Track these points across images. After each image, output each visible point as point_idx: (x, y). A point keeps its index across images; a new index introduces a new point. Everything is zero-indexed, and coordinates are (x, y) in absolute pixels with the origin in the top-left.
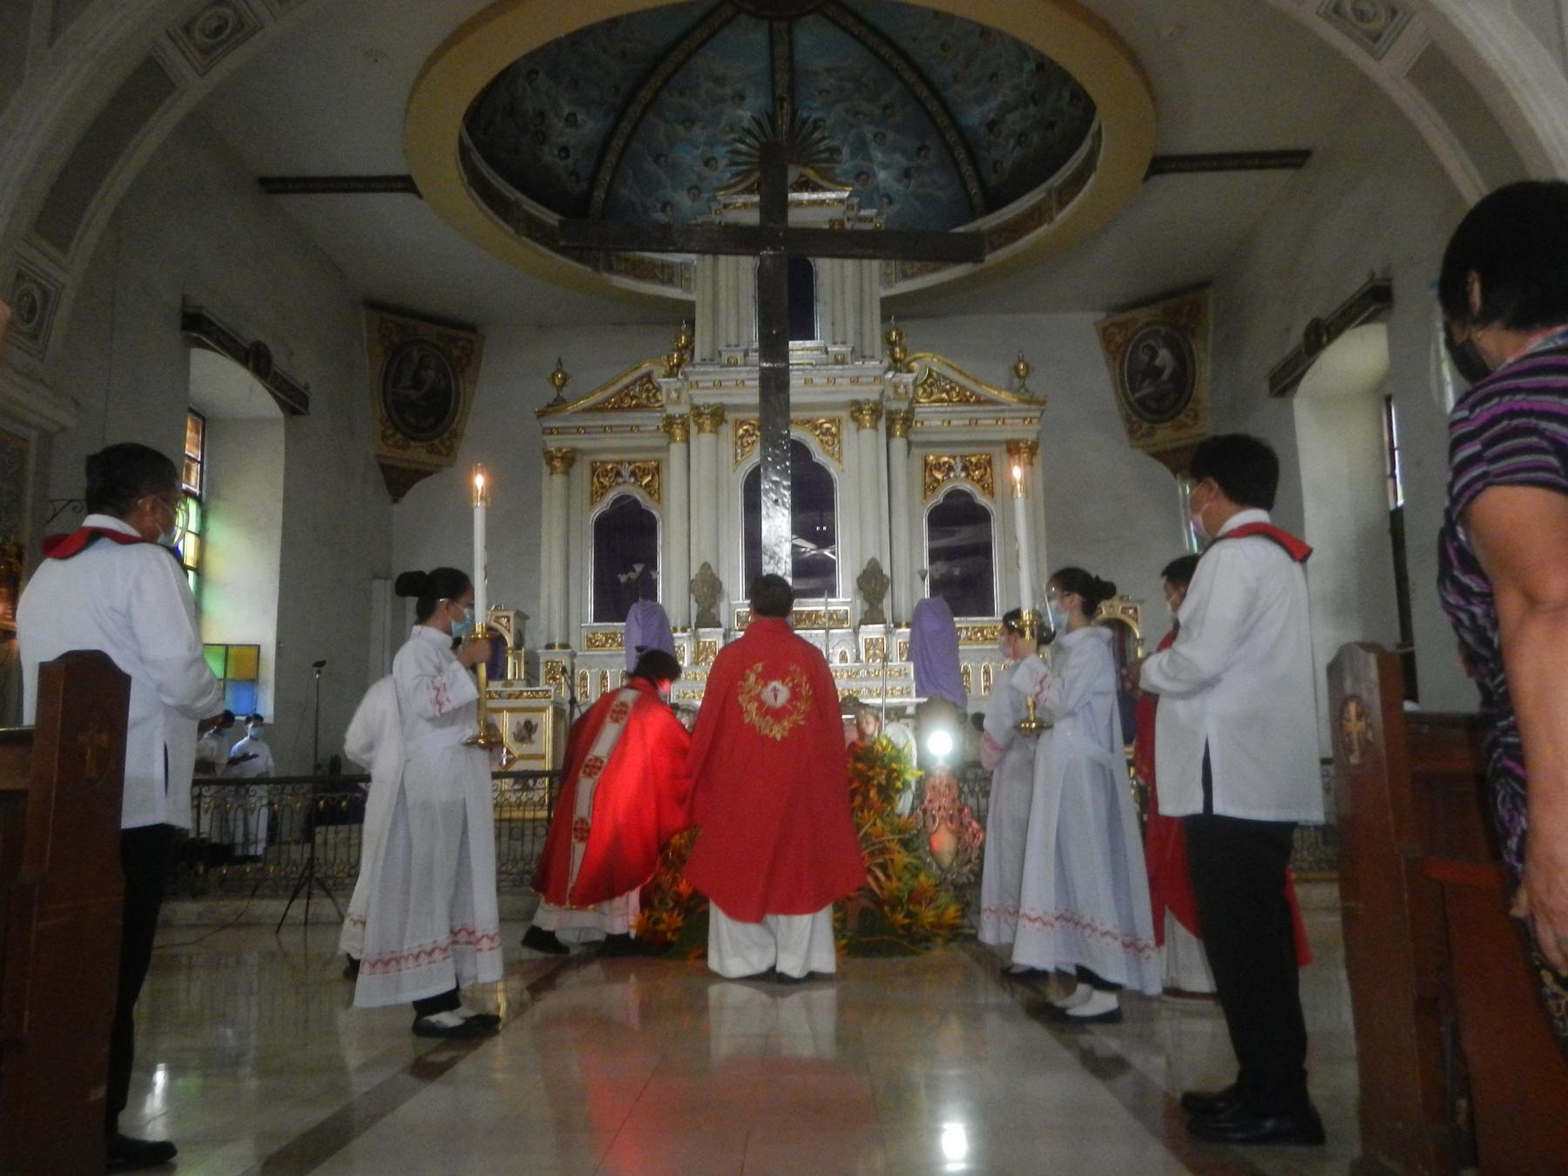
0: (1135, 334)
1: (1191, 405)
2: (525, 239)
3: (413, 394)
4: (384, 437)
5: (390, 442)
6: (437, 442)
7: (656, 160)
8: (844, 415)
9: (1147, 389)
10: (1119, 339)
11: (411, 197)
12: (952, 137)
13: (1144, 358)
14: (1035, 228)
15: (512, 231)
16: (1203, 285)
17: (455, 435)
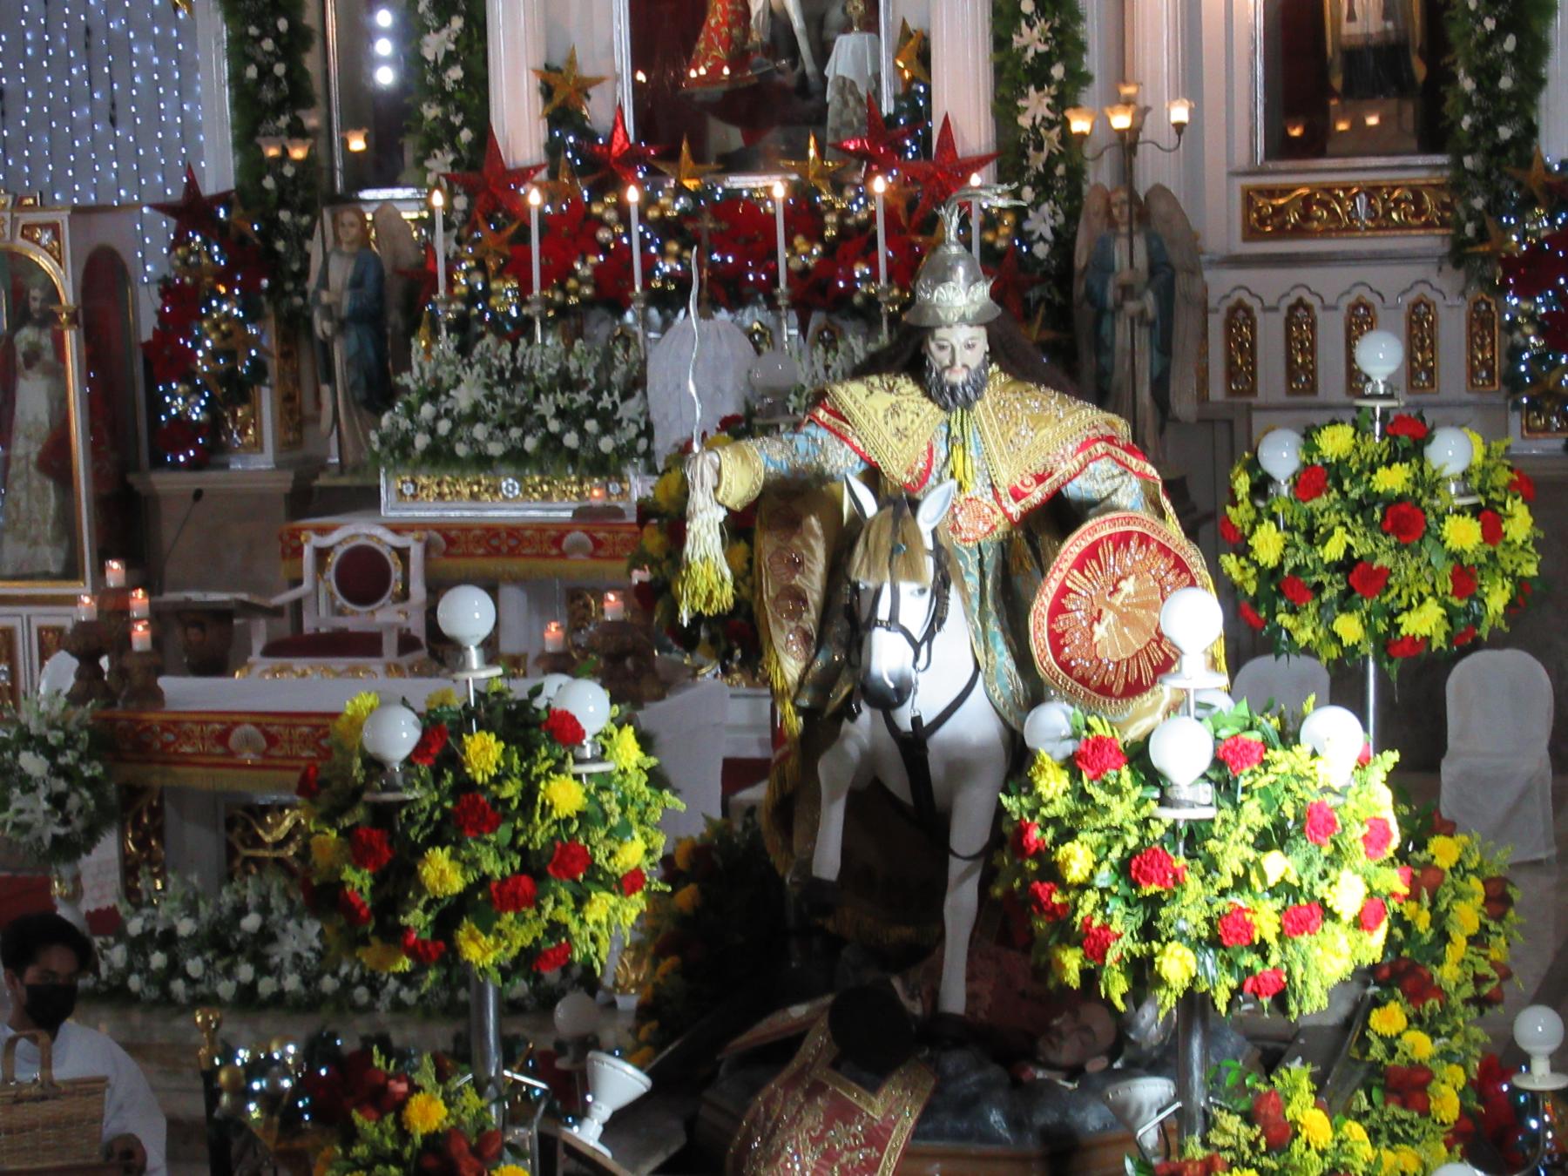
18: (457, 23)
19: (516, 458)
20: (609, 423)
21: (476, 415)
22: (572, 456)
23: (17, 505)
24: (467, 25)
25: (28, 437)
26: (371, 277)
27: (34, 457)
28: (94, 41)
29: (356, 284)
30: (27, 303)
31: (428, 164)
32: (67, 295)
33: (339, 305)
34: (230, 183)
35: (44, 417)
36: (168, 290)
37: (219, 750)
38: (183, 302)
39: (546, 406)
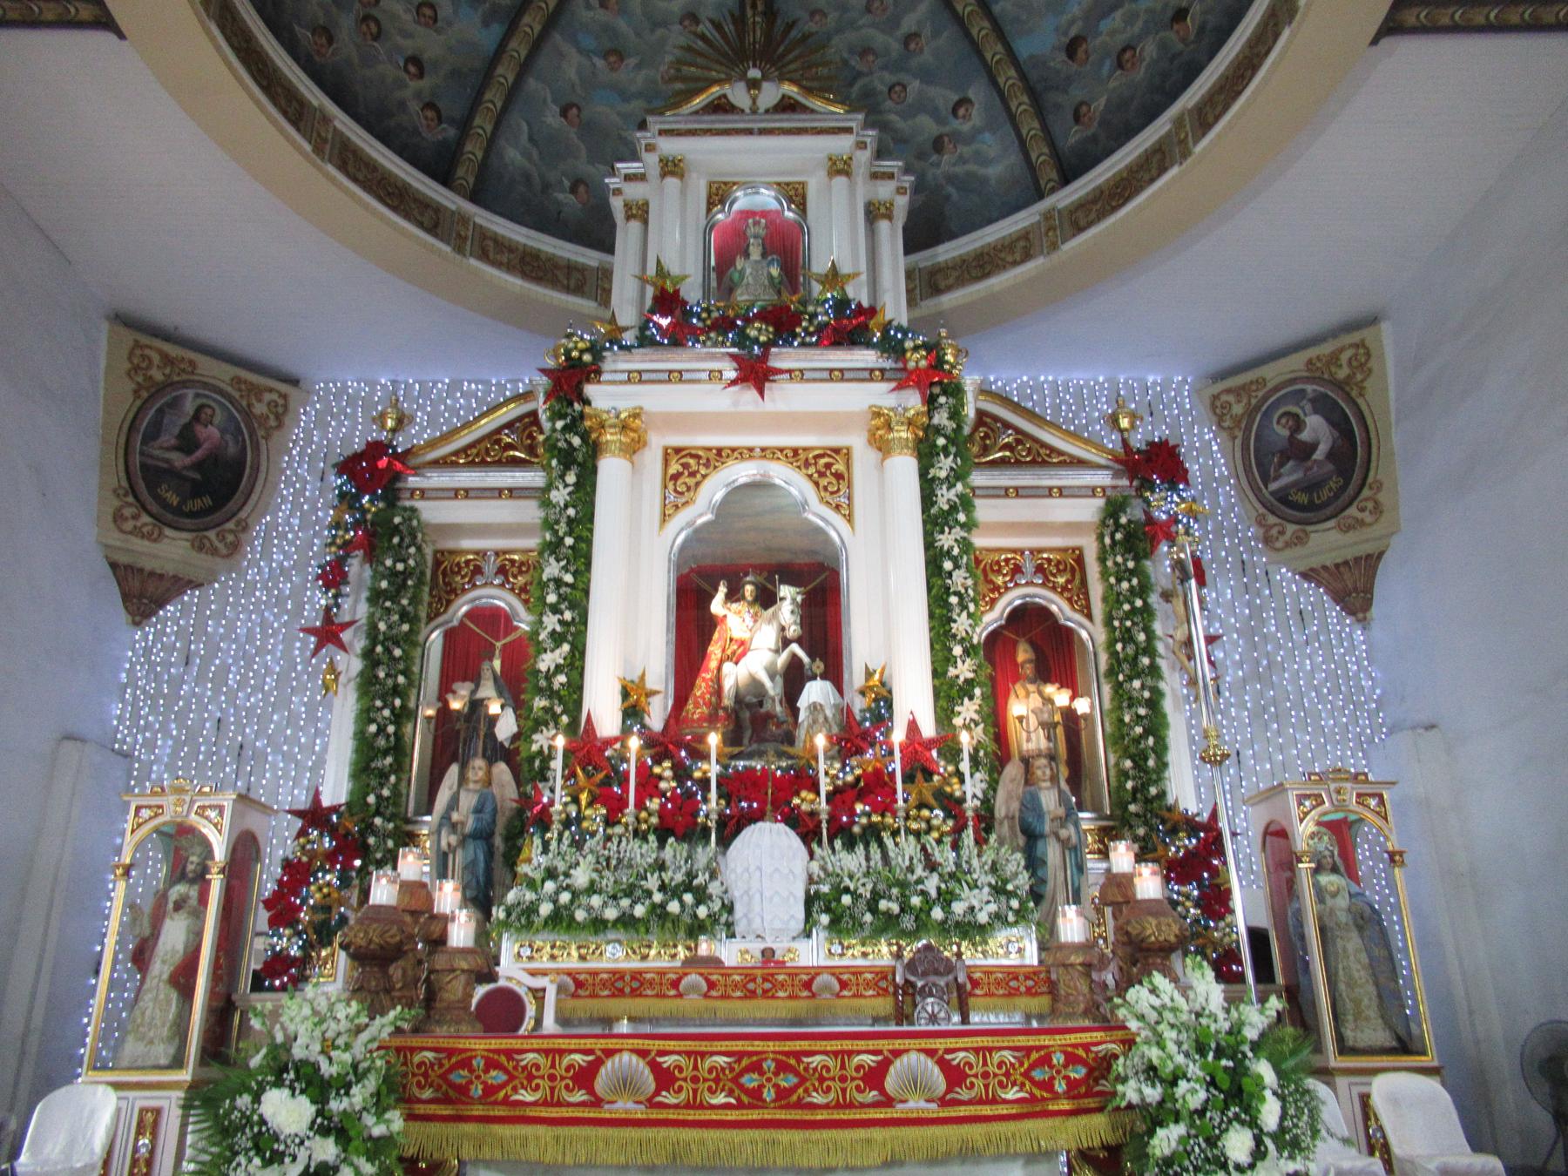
0: (1265, 398)
1: (1366, 492)
2: (331, 169)
3: (179, 460)
4: (118, 517)
5: (129, 525)
6: (212, 534)
7: (564, 113)
8: (857, 442)
9: (1290, 475)
10: (1238, 409)
11: (104, 39)
12: (1008, 77)
13: (1285, 433)
14: (1152, 180)
15: (308, 148)
16: (1373, 320)
17: (244, 527)
18: (566, 647)
19: (627, 921)
20: (702, 896)
21: (592, 889)
22: (676, 920)
23: (143, 1014)
24: (572, 651)
25: (164, 962)
26: (488, 808)
27: (165, 976)
28: (243, 753)
29: (478, 810)
30: (184, 867)
31: (535, 737)
32: (220, 852)
33: (463, 824)
34: (343, 799)
35: (180, 947)
36: (287, 865)
37: (580, 1096)
38: (297, 873)
39: (652, 882)
